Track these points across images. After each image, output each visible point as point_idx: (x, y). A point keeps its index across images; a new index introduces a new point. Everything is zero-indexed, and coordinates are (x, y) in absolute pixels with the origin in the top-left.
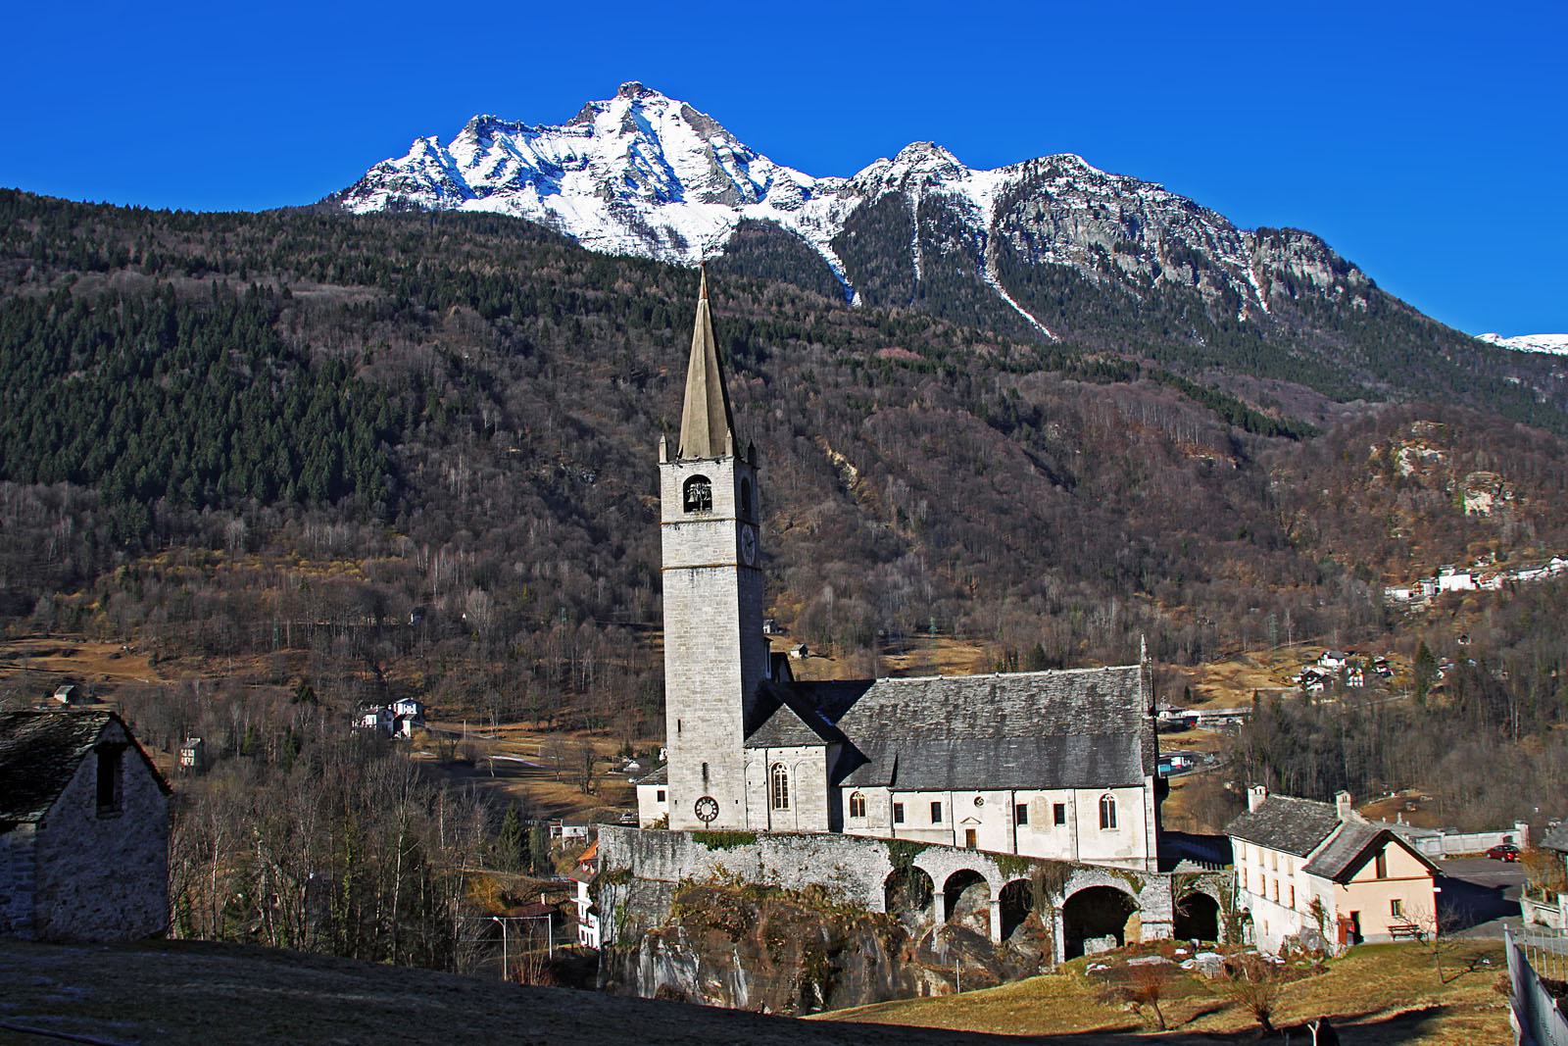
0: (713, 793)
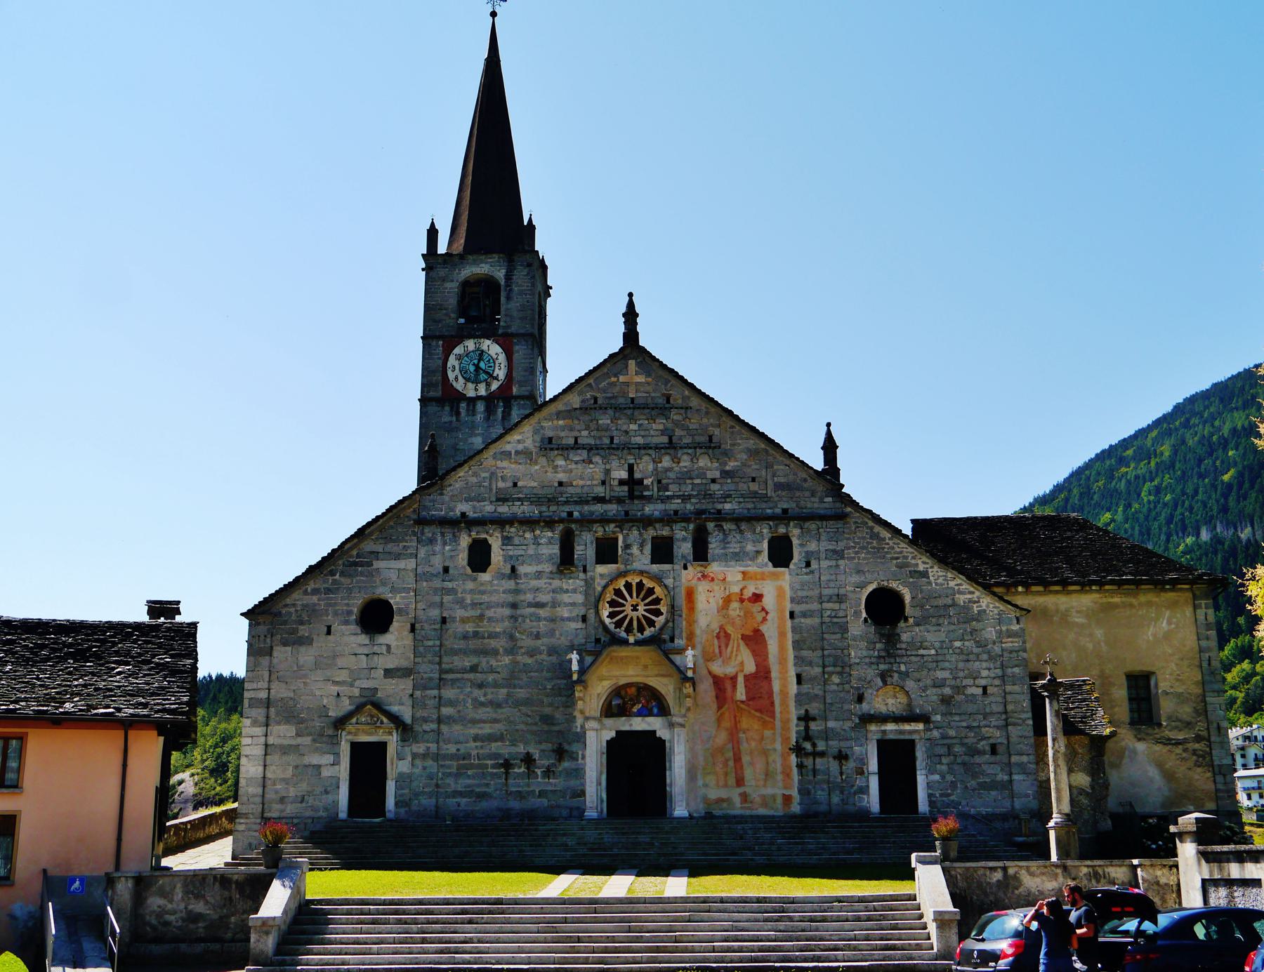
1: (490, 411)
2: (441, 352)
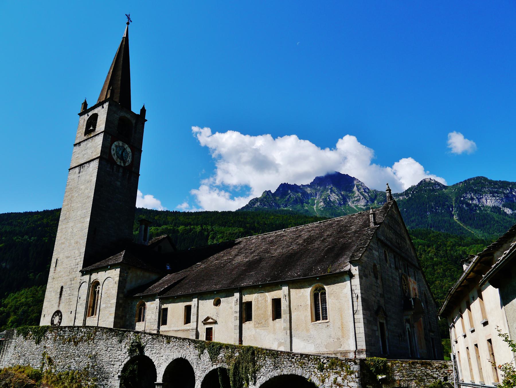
0: (61, 309)
2: (110, 141)
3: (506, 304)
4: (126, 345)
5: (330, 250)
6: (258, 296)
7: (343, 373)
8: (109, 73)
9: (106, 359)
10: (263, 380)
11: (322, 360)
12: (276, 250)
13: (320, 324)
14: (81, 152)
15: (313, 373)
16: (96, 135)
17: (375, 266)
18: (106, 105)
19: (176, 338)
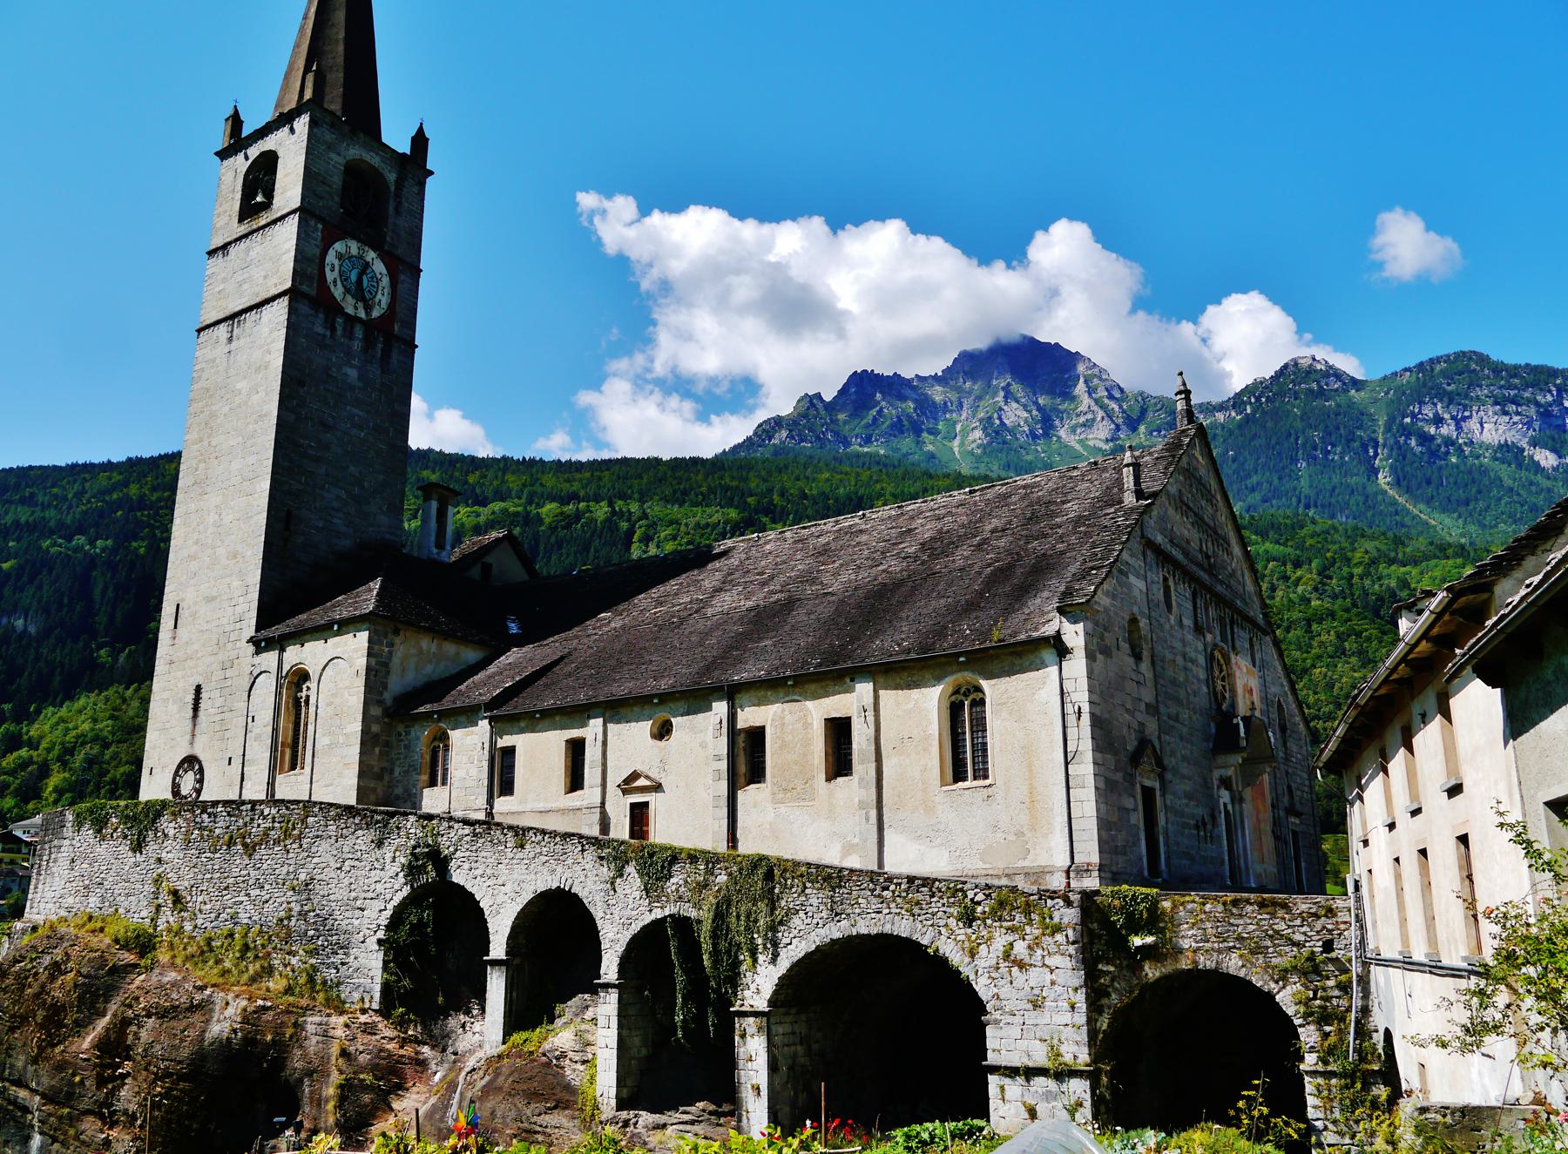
0: (199, 751)
1: (369, 342)
3: (1520, 734)
4: (398, 854)
5: (1003, 574)
6: (783, 711)
7: (1033, 931)
8: (305, 17)
9: (340, 893)
10: (799, 950)
11: (970, 894)
12: (836, 574)
13: (966, 792)
14: (230, 275)
15: (943, 930)
16: (275, 222)
17: (1134, 621)
18: (302, 124)
19: (544, 832)
